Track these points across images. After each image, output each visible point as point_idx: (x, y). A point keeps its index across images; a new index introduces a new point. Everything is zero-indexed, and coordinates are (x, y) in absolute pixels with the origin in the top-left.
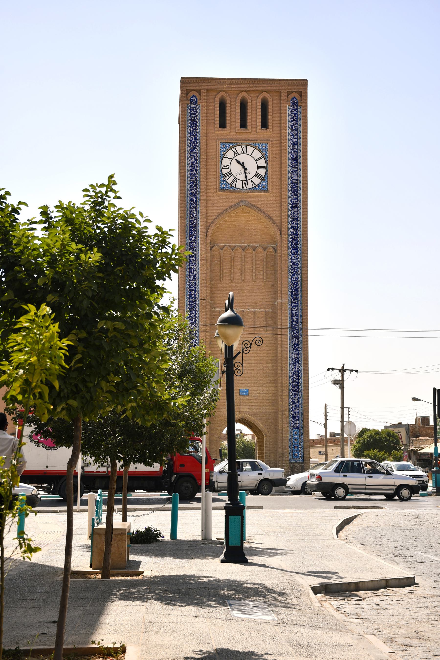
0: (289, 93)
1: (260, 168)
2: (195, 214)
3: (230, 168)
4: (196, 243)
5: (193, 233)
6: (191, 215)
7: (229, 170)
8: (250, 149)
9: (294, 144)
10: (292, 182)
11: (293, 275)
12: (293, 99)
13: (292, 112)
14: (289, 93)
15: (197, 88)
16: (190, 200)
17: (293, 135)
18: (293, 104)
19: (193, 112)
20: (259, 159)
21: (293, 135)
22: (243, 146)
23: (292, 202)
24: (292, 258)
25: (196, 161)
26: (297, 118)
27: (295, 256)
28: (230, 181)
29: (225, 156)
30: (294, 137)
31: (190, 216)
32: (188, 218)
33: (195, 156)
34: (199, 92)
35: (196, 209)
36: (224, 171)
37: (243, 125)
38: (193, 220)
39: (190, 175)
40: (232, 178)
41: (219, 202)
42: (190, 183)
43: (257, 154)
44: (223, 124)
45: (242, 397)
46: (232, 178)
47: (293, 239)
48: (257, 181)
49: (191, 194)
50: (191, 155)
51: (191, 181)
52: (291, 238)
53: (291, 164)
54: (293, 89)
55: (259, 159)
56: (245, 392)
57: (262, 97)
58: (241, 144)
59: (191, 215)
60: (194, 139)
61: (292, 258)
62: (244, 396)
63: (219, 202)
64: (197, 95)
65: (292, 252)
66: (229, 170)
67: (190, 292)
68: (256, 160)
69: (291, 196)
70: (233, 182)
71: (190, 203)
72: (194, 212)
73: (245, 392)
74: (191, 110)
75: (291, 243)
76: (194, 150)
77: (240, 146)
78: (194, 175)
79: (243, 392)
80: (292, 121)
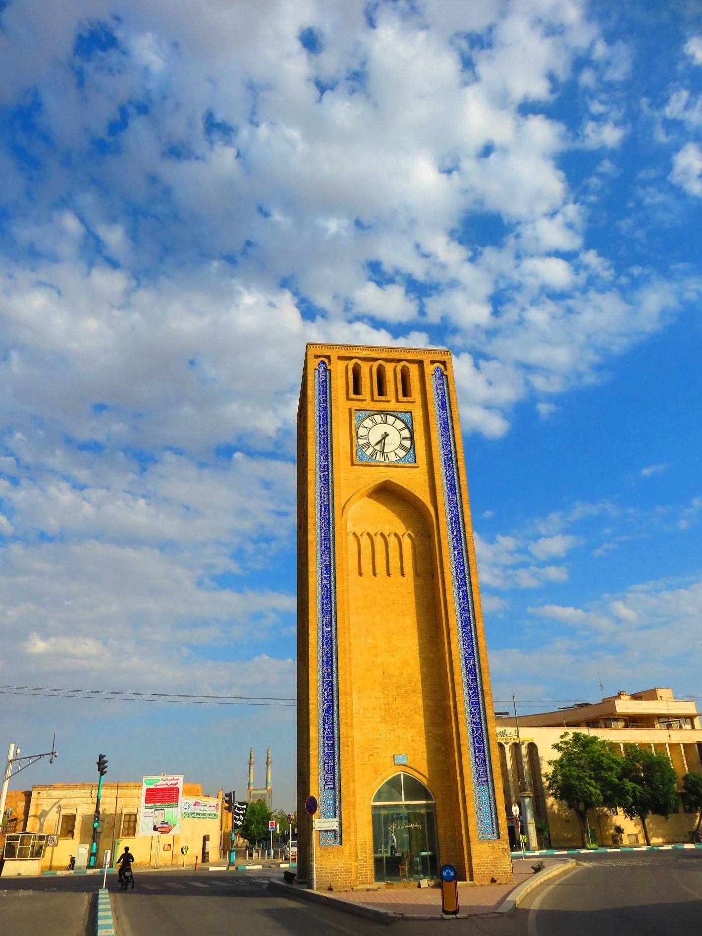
1: (405, 439)
8: (391, 419)
14: (433, 362)
34: (328, 357)
36: (361, 442)
37: (382, 391)
44: (357, 390)
48: (402, 453)
58: (380, 412)
64: (326, 361)
70: (372, 455)
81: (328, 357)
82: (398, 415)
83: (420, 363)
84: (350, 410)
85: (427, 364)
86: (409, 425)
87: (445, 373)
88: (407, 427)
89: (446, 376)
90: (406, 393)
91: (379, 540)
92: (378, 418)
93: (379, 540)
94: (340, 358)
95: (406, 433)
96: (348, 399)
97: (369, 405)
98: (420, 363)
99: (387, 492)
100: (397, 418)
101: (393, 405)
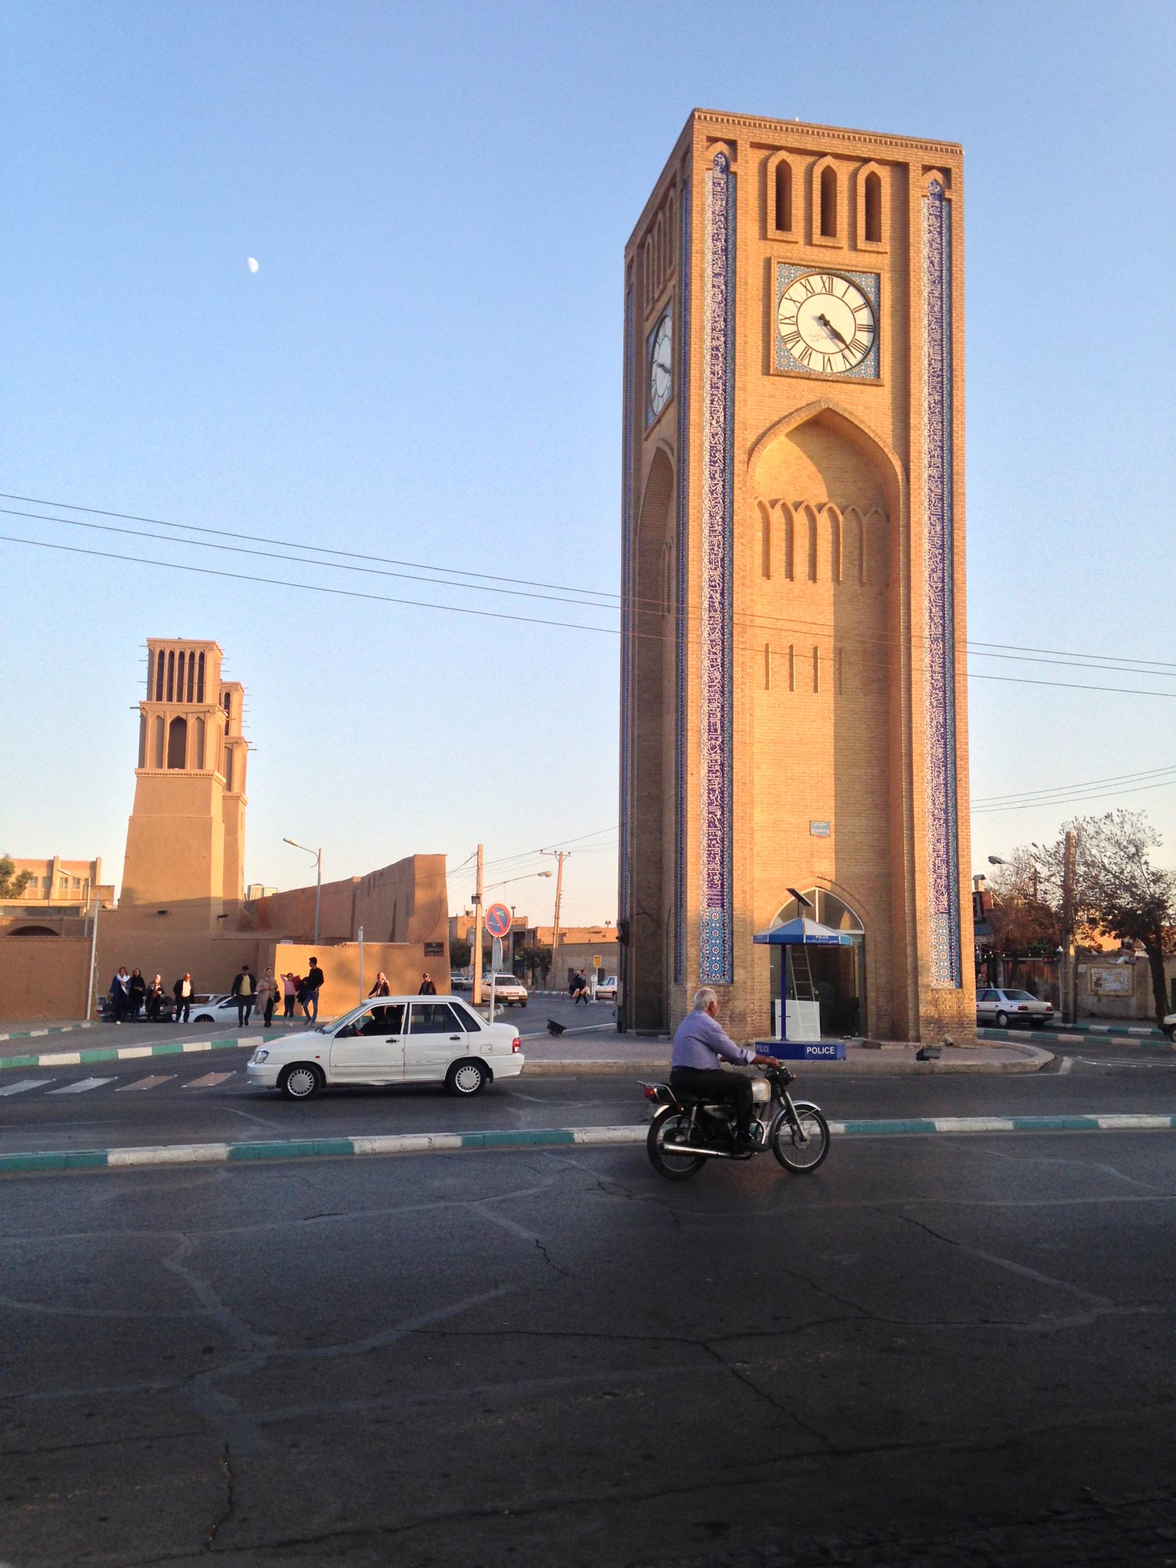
0: (927, 169)
2: (722, 419)
3: (796, 324)
4: (724, 487)
5: (715, 462)
7: (794, 328)
8: (840, 285)
10: (930, 365)
11: (932, 570)
14: (927, 169)
15: (731, 137)
17: (932, 262)
19: (719, 189)
20: (859, 309)
21: (932, 262)
22: (825, 277)
26: (941, 227)
27: (938, 528)
28: (797, 351)
33: (723, 287)
34: (732, 144)
35: (724, 409)
36: (785, 330)
37: (828, 229)
40: (801, 346)
41: (773, 396)
44: (783, 223)
45: (815, 839)
46: (801, 346)
49: (713, 373)
51: (715, 343)
55: (859, 309)
56: (823, 827)
57: (868, 172)
59: (714, 422)
62: (820, 837)
63: (773, 396)
66: (794, 328)
67: (711, 597)
68: (854, 312)
70: (803, 356)
73: (823, 827)
75: (930, 500)
77: (818, 277)
79: (818, 827)
80: (930, 232)
81: (732, 144)
82: (856, 278)
83: (901, 168)
84: (768, 262)
85: (914, 173)
86: (872, 298)
87: (947, 195)
88: (868, 303)
89: (949, 201)
90: (872, 234)
91: (800, 518)
92: (816, 281)
93: (800, 518)
94: (756, 146)
95: (864, 317)
96: (764, 236)
97: (801, 251)
98: (901, 168)
99: (826, 430)
100: (851, 283)
101: (845, 258)
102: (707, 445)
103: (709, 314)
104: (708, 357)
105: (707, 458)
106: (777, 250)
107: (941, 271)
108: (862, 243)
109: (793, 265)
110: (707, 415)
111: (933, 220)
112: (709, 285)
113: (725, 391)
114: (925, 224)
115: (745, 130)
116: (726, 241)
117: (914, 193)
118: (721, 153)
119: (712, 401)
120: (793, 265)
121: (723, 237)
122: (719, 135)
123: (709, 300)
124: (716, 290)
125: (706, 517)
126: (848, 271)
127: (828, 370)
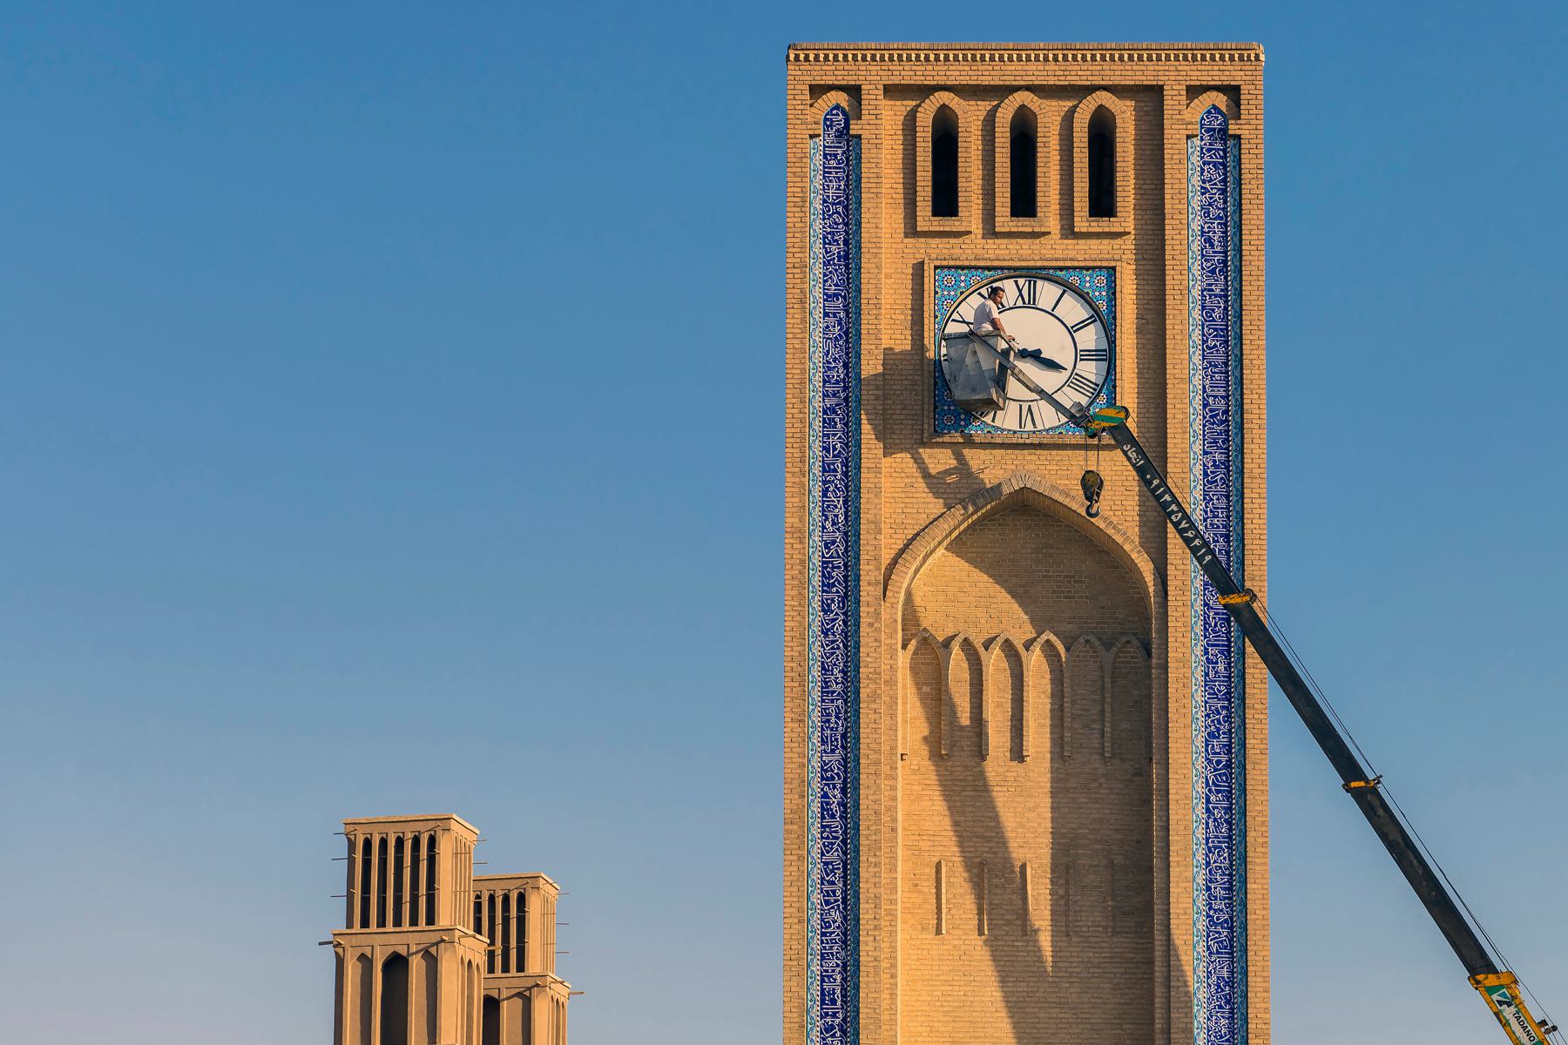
0: (1194, 91)
4: (845, 623)
6: (828, 525)
8: (1047, 292)
9: (1213, 272)
10: (1205, 406)
12: (1209, 112)
13: (1207, 159)
14: (1194, 91)
15: (851, 80)
16: (824, 471)
17: (1209, 241)
18: (1208, 131)
19: (833, 163)
20: (1082, 325)
21: (1209, 241)
22: (1021, 281)
23: (1206, 474)
24: (1207, 674)
25: (847, 333)
26: (1224, 181)
27: (1221, 667)
29: (955, 316)
30: (1212, 245)
31: (824, 527)
32: (818, 532)
33: (842, 315)
34: (854, 91)
35: (845, 502)
38: (833, 543)
39: (825, 382)
42: (825, 412)
43: (1073, 310)
44: (946, 203)
47: (1210, 608)
49: (826, 449)
50: (826, 315)
51: (830, 402)
52: (1206, 604)
53: (1204, 342)
54: (1206, 80)
55: (1082, 325)
57: (1093, 107)
58: (1015, 272)
59: (828, 525)
60: (839, 258)
61: (1207, 674)
65: (1206, 653)
68: (1072, 331)
69: (1205, 453)
71: (825, 482)
72: (840, 512)
74: (825, 156)
76: (836, 295)
77: (1011, 281)
78: (837, 382)
80: (1204, 191)
81: (854, 91)
82: (1074, 278)
83: (1150, 97)
84: (919, 269)
85: (1174, 101)
87: (1233, 129)
88: (1096, 316)
90: (1103, 204)
94: (892, 91)
95: (1090, 338)
96: (912, 231)
97: (976, 248)
98: (1150, 97)
100: (1067, 287)
101: (1055, 249)
102: (816, 560)
103: (818, 357)
104: (817, 425)
105: (817, 580)
106: (938, 249)
107: (1225, 252)
108: (1082, 222)
109: (963, 268)
110: (817, 513)
111: (1210, 172)
112: (818, 314)
113: (845, 474)
114: (1196, 180)
115: (874, 68)
116: (846, 242)
117: (1173, 134)
118: (837, 107)
119: (825, 493)
120: (963, 268)
121: (841, 238)
122: (830, 80)
123: (818, 336)
124: (831, 320)
125: (816, 672)
126: (1061, 269)
127: (1029, 427)
